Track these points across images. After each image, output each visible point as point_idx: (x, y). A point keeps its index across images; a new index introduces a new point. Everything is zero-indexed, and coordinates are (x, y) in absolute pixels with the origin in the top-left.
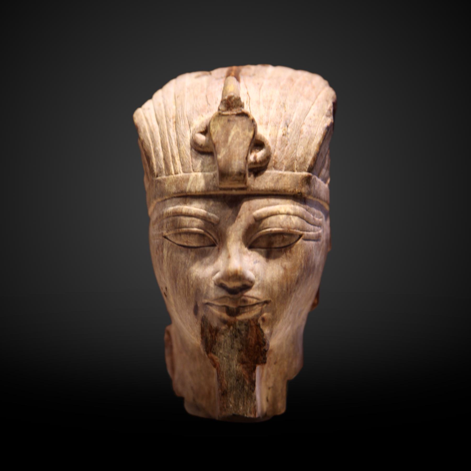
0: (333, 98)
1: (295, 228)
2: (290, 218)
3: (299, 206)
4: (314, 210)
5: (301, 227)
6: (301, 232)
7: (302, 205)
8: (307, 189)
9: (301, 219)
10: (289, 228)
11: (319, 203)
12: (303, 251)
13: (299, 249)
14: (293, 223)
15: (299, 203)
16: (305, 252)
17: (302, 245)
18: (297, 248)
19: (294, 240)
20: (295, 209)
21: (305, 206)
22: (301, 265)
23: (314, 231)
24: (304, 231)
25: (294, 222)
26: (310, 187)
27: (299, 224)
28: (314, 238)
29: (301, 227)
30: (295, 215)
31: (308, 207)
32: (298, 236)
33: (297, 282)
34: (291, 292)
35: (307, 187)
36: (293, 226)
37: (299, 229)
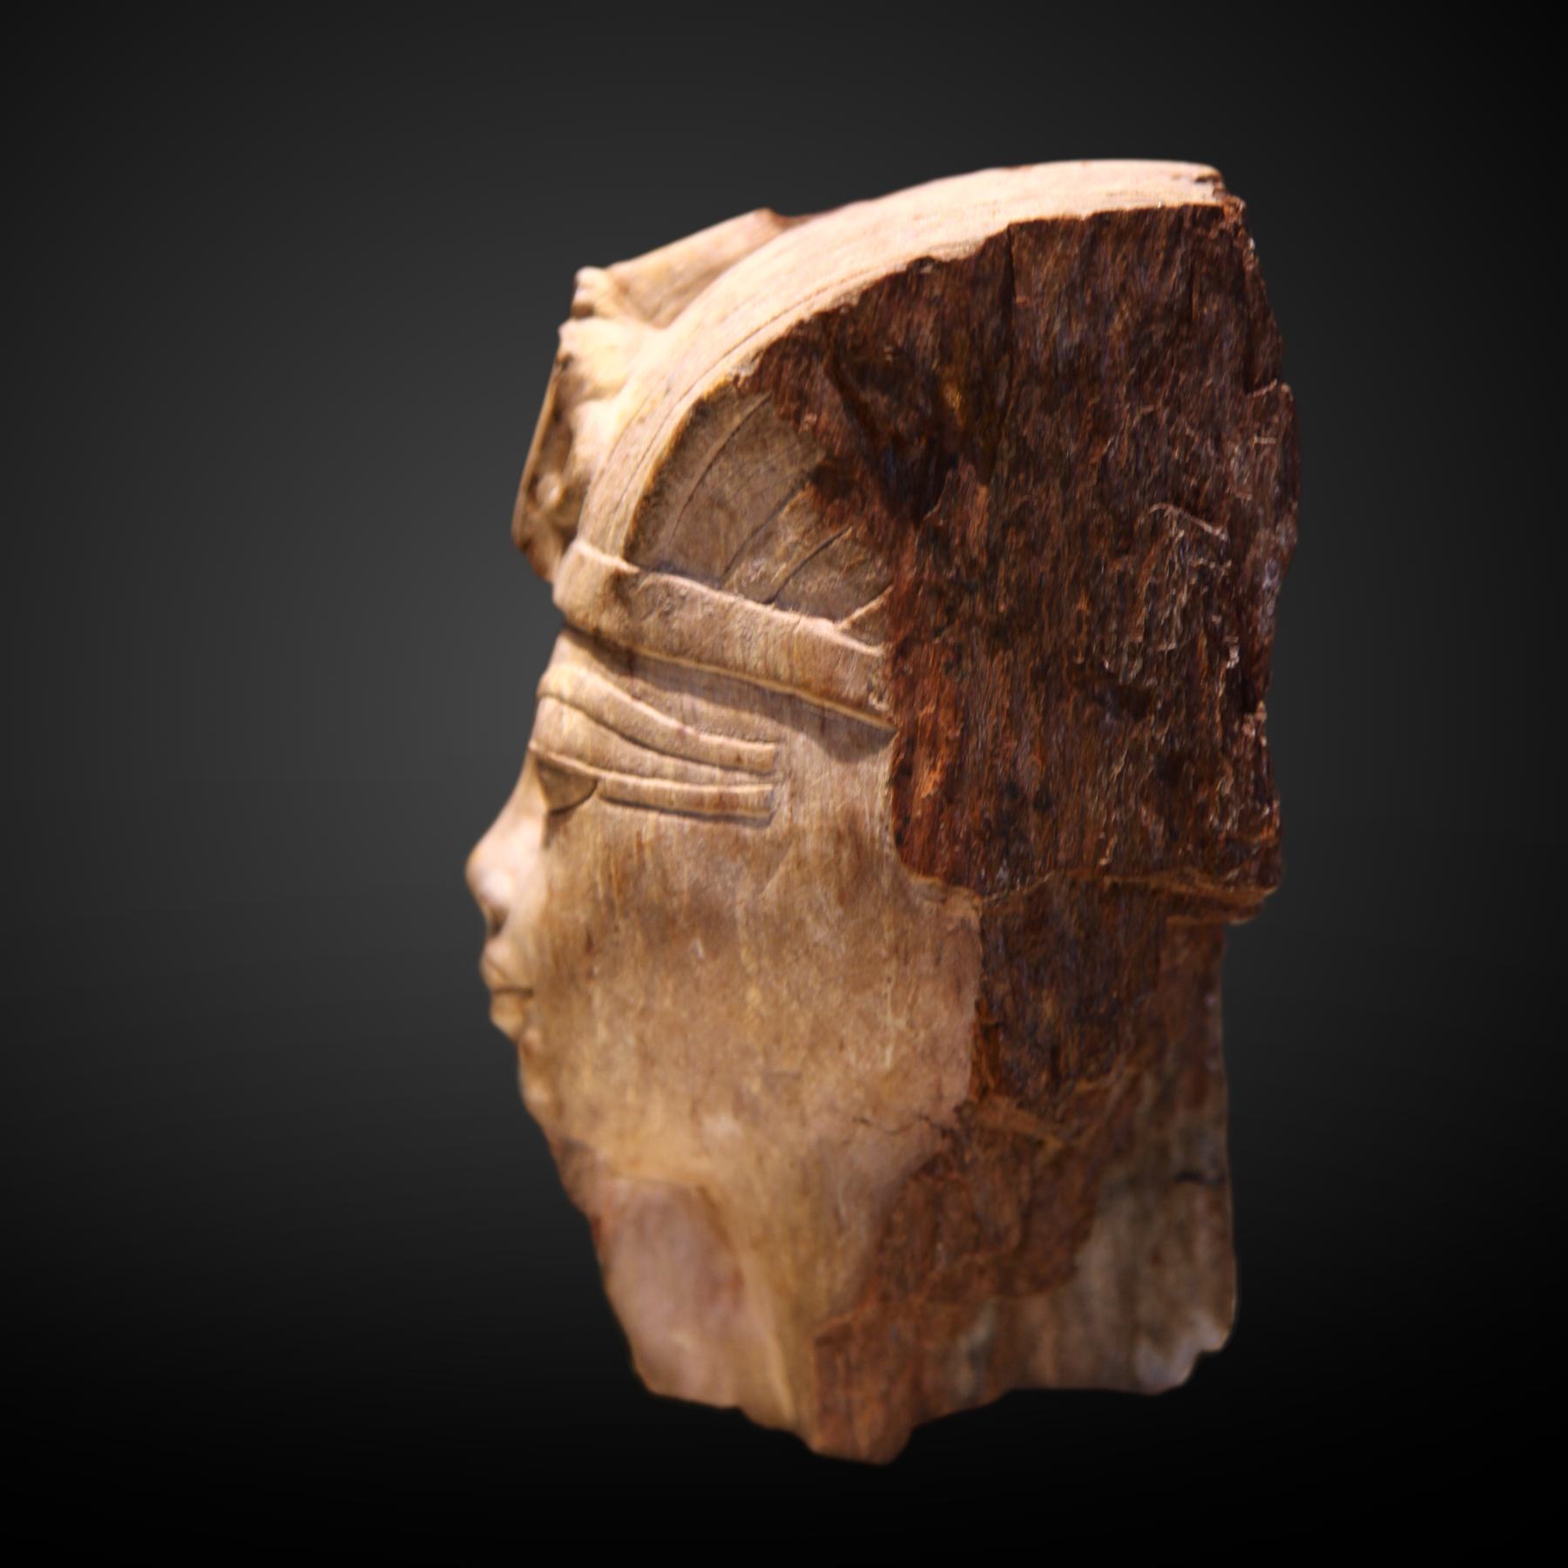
0: (847, 294)
1: (564, 751)
2: (561, 714)
3: (605, 676)
4: (687, 701)
5: (589, 754)
6: (592, 771)
7: (614, 677)
8: (621, 621)
9: (592, 724)
10: (548, 748)
11: (757, 688)
12: (599, 839)
13: (587, 828)
14: (559, 731)
15: (603, 668)
16: (607, 846)
17: (595, 816)
18: (581, 824)
19: (577, 796)
20: (581, 684)
21: (626, 681)
22: (594, 887)
23: (680, 777)
24: (608, 767)
25: (566, 730)
26: (631, 614)
27: (580, 741)
28: (676, 806)
29: (589, 754)
30: (576, 705)
31: (639, 685)
32: (590, 785)
33: (589, 946)
34: (573, 977)
35: (617, 610)
36: (558, 742)
37: (580, 757)
